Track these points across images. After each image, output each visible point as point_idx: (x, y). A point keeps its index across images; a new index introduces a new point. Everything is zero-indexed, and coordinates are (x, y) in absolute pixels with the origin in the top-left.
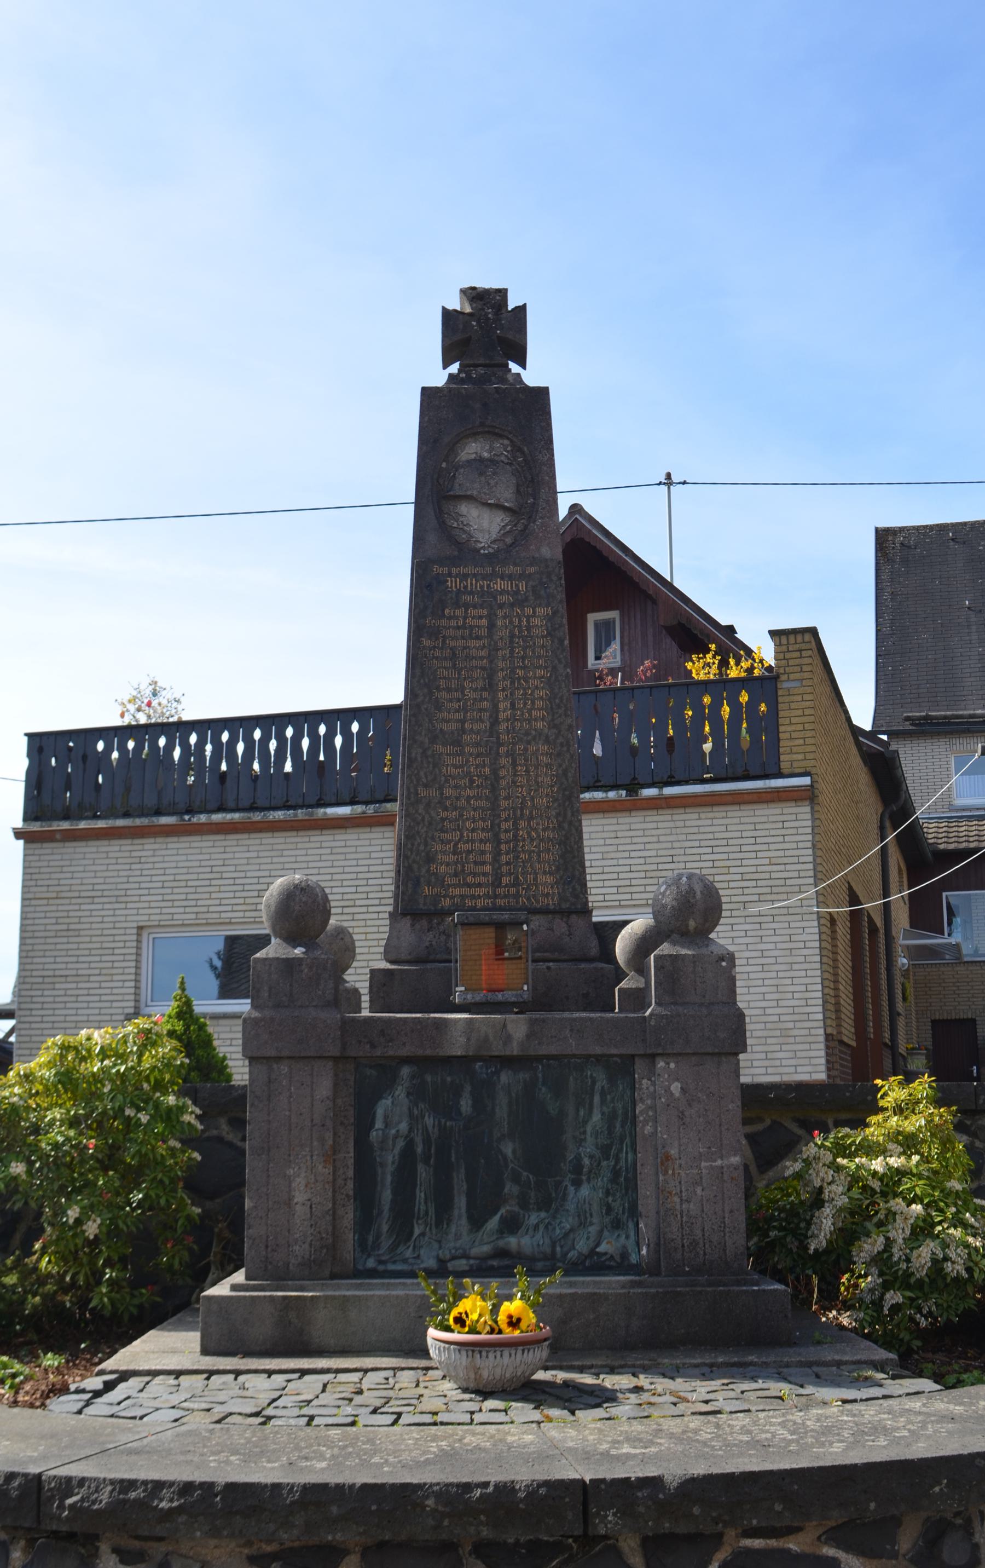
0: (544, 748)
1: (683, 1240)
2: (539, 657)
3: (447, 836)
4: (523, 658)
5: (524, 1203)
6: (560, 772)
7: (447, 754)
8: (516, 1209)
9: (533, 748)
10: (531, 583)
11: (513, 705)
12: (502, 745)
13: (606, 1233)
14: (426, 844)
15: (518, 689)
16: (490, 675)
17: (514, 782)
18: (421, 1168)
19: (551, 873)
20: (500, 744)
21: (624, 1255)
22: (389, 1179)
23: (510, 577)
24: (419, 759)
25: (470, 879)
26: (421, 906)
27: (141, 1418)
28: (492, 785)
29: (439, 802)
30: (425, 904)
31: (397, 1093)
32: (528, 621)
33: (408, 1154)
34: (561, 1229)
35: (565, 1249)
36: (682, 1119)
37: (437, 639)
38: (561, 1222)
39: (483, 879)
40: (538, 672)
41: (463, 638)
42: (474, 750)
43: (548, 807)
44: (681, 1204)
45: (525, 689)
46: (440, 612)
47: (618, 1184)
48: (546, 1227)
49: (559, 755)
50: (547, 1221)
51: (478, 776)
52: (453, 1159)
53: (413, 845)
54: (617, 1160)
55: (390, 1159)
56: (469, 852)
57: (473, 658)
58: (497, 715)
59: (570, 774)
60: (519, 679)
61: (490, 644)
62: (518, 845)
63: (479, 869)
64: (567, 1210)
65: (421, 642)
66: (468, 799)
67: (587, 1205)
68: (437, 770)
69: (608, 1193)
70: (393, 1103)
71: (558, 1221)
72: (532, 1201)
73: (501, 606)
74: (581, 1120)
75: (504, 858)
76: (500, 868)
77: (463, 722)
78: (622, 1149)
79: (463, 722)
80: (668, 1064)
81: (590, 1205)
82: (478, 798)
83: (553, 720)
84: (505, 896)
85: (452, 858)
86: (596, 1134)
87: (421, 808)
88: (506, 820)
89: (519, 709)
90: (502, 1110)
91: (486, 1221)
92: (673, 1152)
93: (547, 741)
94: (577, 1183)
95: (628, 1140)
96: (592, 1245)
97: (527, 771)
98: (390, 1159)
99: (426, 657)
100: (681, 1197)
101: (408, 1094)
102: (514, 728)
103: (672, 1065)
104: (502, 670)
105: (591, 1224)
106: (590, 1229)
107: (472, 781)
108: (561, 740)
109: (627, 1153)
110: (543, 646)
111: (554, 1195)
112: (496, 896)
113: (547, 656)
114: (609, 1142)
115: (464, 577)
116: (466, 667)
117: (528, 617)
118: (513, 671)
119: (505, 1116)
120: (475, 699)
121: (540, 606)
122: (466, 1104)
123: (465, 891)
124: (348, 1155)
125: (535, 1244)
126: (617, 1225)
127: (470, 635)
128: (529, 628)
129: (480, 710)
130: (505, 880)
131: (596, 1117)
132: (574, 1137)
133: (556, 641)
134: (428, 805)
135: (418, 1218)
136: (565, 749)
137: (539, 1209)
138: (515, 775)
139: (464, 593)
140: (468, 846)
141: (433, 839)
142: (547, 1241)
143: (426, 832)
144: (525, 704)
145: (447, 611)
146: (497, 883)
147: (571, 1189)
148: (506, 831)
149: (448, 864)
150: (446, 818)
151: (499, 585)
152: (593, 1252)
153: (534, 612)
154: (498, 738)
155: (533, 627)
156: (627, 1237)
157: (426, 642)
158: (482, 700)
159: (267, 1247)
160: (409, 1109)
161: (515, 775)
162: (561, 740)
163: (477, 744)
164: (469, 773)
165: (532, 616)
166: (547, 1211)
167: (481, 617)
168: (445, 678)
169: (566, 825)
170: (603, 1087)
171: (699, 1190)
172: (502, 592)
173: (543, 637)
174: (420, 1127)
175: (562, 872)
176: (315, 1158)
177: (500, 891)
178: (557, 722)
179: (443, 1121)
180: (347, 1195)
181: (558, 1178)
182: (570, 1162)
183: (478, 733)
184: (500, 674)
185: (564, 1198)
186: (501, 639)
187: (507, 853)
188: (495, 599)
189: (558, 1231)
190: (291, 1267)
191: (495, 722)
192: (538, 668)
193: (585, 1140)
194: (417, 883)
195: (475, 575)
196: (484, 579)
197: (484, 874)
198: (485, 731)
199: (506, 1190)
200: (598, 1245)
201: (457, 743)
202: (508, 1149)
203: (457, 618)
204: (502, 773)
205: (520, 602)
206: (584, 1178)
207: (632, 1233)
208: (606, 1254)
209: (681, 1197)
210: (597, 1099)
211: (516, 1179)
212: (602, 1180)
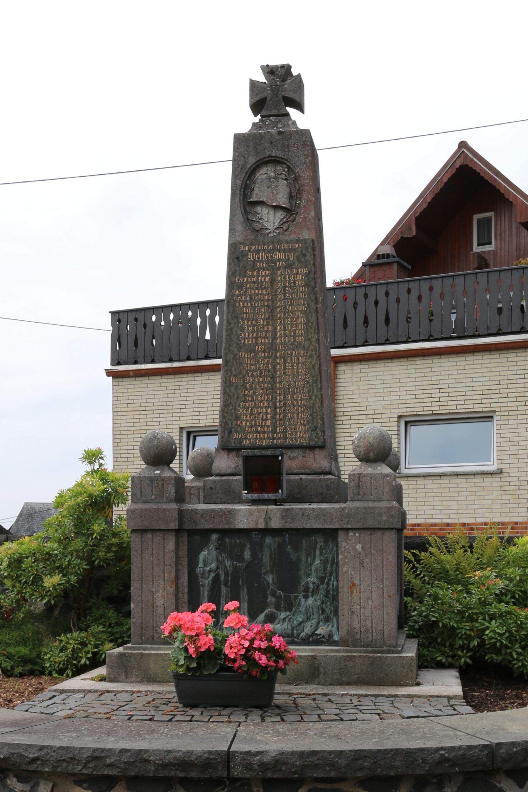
0: (301, 352)
1: (360, 628)
2: (300, 298)
3: (247, 405)
4: (291, 299)
5: (278, 608)
6: (311, 366)
7: (247, 358)
8: (274, 610)
9: (295, 353)
10: (297, 254)
11: (285, 328)
12: (278, 351)
13: (321, 624)
14: (235, 409)
15: (288, 318)
16: (272, 309)
17: (285, 373)
18: (223, 588)
19: (304, 425)
20: (277, 351)
21: (330, 635)
22: (206, 593)
23: (284, 251)
24: (232, 361)
25: (259, 429)
26: (233, 445)
27: (52, 714)
28: (272, 374)
29: (243, 385)
30: (234, 443)
31: (210, 548)
32: (294, 277)
33: (216, 581)
34: (297, 621)
35: (299, 632)
36: (362, 564)
37: (242, 290)
38: (297, 618)
39: (267, 429)
40: (299, 307)
41: (257, 289)
42: (263, 355)
43: (304, 387)
44: (360, 609)
45: (291, 318)
46: (244, 274)
47: (328, 598)
48: (289, 620)
49: (310, 356)
50: (290, 617)
51: (264, 370)
52: (240, 583)
53: (228, 410)
54: (328, 584)
55: (207, 582)
56: (259, 414)
57: (263, 300)
58: (276, 334)
59: (316, 368)
60: (288, 312)
61: (272, 292)
62: (286, 409)
63: (265, 423)
64: (301, 612)
65: (233, 292)
66: (259, 383)
67: (311, 609)
68: (241, 367)
69: (323, 602)
70: (208, 554)
71: (296, 617)
72: (282, 606)
73: (279, 269)
74: (309, 563)
75: (278, 417)
76: (276, 422)
77: (256, 338)
78: (331, 579)
79: (256, 338)
80: (355, 534)
81: (313, 609)
82: (264, 382)
83: (307, 336)
84: (279, 438)
85: (249, 417)
86: (317, 571)
87: (233, 389)
88: (280, 395)
89: (288, 330)
90: (266, 558)
91: (258, 616)
92: (357, 582)
93: (304, 348)
94: (306, 597)
95: (334, 574)
96: (314, 630)
97: (292, 366)
98: (207, 582)
99: (236, 301)
100: (360, 606)
101: (216, 549)
102: (285, 341)
103: (357, 535)
104: (278, 307)
105: (313, 619)
106: (313, 621)
107: (261, 373)
108: (312, 347)
109: (333, 581)
110: (302, 292)
111: (294, 603)
112: (274, 438)
113: (305, 298)
114: (324, 575)
115: (258, 251)
116: (258, 306)
117: (294, 275)
118: (285, 308)
119: (268, 561)
120: (263, 325)
121: (301, 267)
122: (247, 555)
123: (257, 436)
124: (184, 580)
125: (283, 629)
126: (327, 620)
127: (261, 287)
128: (294, 282)
129: (267, 331)
130: (279, 429)
131: (317, 562)
132: (305, 573)
133: (310, 288)
134: (236, 387)
135: (222, 614)
136: (314, 353)
137: (286, 610)
138: (285, 369)
139: (257, 261)
140: (259, 410)
141: (239, 406)
142: (290, 627)
143: (235, 403)
144: (292, 327)
145: (248, 273)
146: (274, 431)
147: (303, 600)
148: (280, 401)
149: (247, 421)
150: (247, 394)
151: (278, 255)
152: (313, 634)
153: (298, 271)
154: (276, 347)
155: (297, 280)
156: (333, 626)
157: (236, 292)
158: (268, 325)
159: (142, 628)
160: (217, 557)
161: (285, 369)
162: (312, 347)
163: (264, 351)
164: (259, 368)
165: (297, 274)
166: (290, 611)
167: (267, 276)
168: (246, 313)
169: (313, 397)
170: (321, 546)
171: (370, 602)
172: (279, 260)
173: (302, 286)
174: (223, 566)
175: (310, 424)
176: (166, 582)
177: (276, 435)
178: (310, 337)
179: (235, 563)
180: (185, 602)
181: (296, 594)
182: (303, 586)
183: (265, 345)
184: (278, 310)
185: (299, 605)
186: (279, 288)
187: (280, 414)
188: (276, 264)
189: (295, 622)
190: (155, 638)
191: (275, 338)
192: (299, 305)
193: (311, 574)
194: (230, 432)
195: (264, 250)
196: (269, 252)
197: (267, 426)
198: (269, 344)
199: (268, 600)
200: (316, 630)
201: (253, 351)
202: (270, 578)
203: (254, 276)
204: (278, 368)
205: (290, 266)
206: (310, 594)
207: (335, 624)
208: (320, 634)
209: (360, 606)
210: (318, 552)
211: (274, 594)
212: (320, 596)
